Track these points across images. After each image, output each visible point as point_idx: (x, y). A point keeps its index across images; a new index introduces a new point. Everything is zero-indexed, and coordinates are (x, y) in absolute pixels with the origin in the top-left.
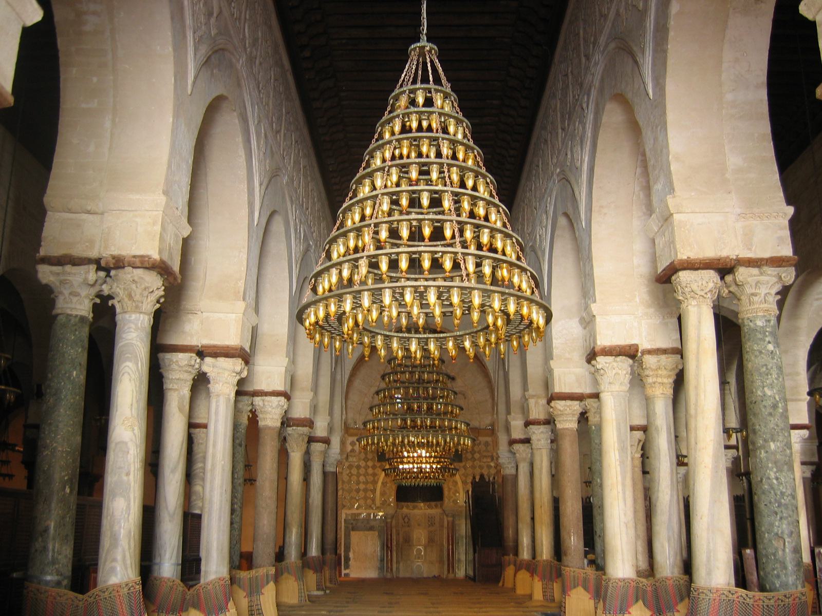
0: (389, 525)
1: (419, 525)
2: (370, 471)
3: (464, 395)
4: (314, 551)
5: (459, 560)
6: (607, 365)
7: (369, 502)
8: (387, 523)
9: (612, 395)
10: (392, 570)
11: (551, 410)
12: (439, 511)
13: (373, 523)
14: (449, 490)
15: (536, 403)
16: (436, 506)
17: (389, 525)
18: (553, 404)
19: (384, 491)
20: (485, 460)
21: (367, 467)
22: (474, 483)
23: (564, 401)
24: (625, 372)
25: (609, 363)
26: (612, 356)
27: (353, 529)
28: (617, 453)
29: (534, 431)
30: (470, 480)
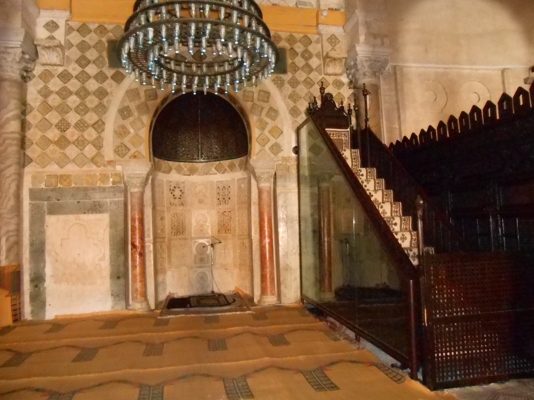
1: (201, 202)
2: (92, 85)
5: (288, 268)
7: (90, 151)
10: (145, 295)
12: (239, 174)
13: (97, 197)
14: (263, 126)
16: (232, 167)
17: (136, 201)
19: (123, 127)
21: (83, 77)
22: (311, 112)
27: (52, 212)
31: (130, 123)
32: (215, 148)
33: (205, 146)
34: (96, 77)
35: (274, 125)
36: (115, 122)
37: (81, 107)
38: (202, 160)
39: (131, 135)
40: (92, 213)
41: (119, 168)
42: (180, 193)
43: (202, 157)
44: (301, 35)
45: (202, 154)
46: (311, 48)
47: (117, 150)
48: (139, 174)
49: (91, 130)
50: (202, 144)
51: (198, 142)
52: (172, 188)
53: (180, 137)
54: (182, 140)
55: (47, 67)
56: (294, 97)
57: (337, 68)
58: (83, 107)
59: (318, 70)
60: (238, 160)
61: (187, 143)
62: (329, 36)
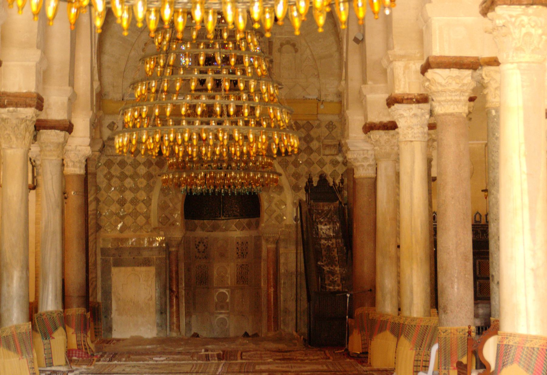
0: (173, 257)
3: (294, 45)
4: (50, 304)
5: (286, 311)
6: (513, 19)
8: (170, 253)
9: (519, 69)
10: (178, 327)
11: (427, 84)
13: (146, 254)
14: (270, 201)
15: (406, 68)
16: (249, 226)
18: (430, 73)
20: (327, 152)
22: (309, 187)
23: (447, 70)
24: (540, 31)
25: (517, 17)
26: (520, 4)
28: (523, 160)
29: (401, 112)
30: (303, 183)
34: (144, 164)
38: (223, 218)
40: (143, 266)
42: (203, 248)
43: (223, 215)
44: (305, 122)
45: (223, 212)
46: (312, 133)
49: (141, 205)
52: (197, 243)
55: (110, 157)
56: (297, 176)
57: (333, 150)
59: (318, 151)
62: (327, 123)
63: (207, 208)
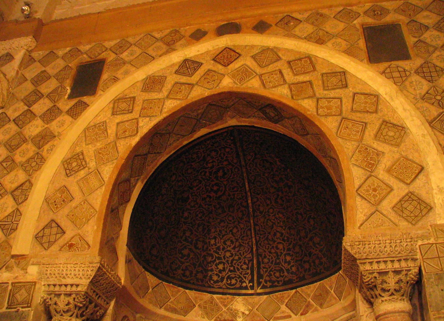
14: (370, 161)
16: (321, 299)
19: (64, 189)
31: (77, 182)
32: (286, 262)
33: (266, 260)
35: (397, 156)
36: (52, 182)
37: (4, 164)
38: (259, 291)
39: (73, 204)
41: (33, 271)
45: (260, 276)
47: (41, 234)
48: (72, 285)
50: (259, 255)
51: (252, 251)
53: (213, 242)
54: (218, 248)
58: (9, 163)
60: (333, 278)
61: (228, 254)
63: (221, 267)
